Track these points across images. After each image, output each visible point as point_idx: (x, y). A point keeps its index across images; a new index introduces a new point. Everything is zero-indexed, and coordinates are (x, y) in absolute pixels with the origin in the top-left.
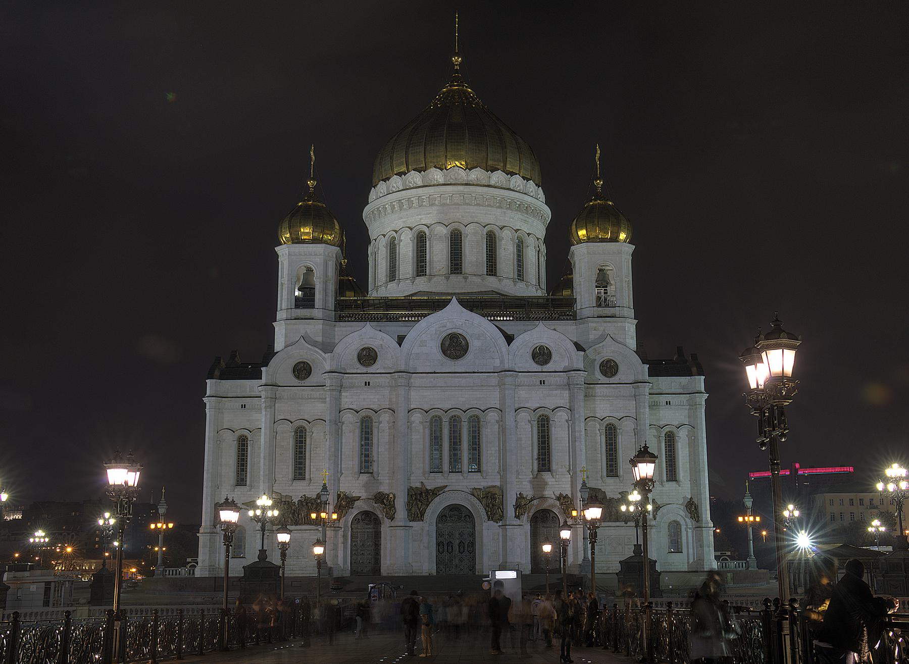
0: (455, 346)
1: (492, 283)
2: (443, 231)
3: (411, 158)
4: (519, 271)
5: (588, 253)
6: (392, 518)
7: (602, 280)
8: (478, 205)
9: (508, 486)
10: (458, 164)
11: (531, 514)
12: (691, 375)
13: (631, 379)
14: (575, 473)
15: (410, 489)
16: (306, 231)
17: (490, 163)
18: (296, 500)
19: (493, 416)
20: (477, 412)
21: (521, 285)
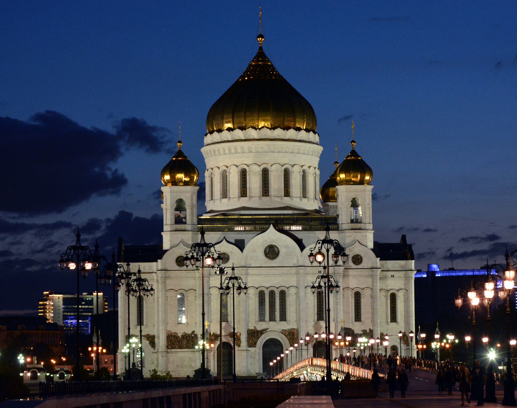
0: (272, 252)
1: (287, 202)
2: (258, 170)
3: (236, 120)
4: (303, 192)
5: (346, 191)
6: (239, 346)
7: (354, 204)
8: (279, 152)
9: (301, 328)
10: (266, 125)
11: (313, 343)
12: (406, 259)
13: (369, 266)
14: (337, 322)
15: (249, 330)
16: (180, 176)
17: (286, 123)
18: (180, 335)
19: (292, 291)
20: (284, 289)
21: (305, 200)
